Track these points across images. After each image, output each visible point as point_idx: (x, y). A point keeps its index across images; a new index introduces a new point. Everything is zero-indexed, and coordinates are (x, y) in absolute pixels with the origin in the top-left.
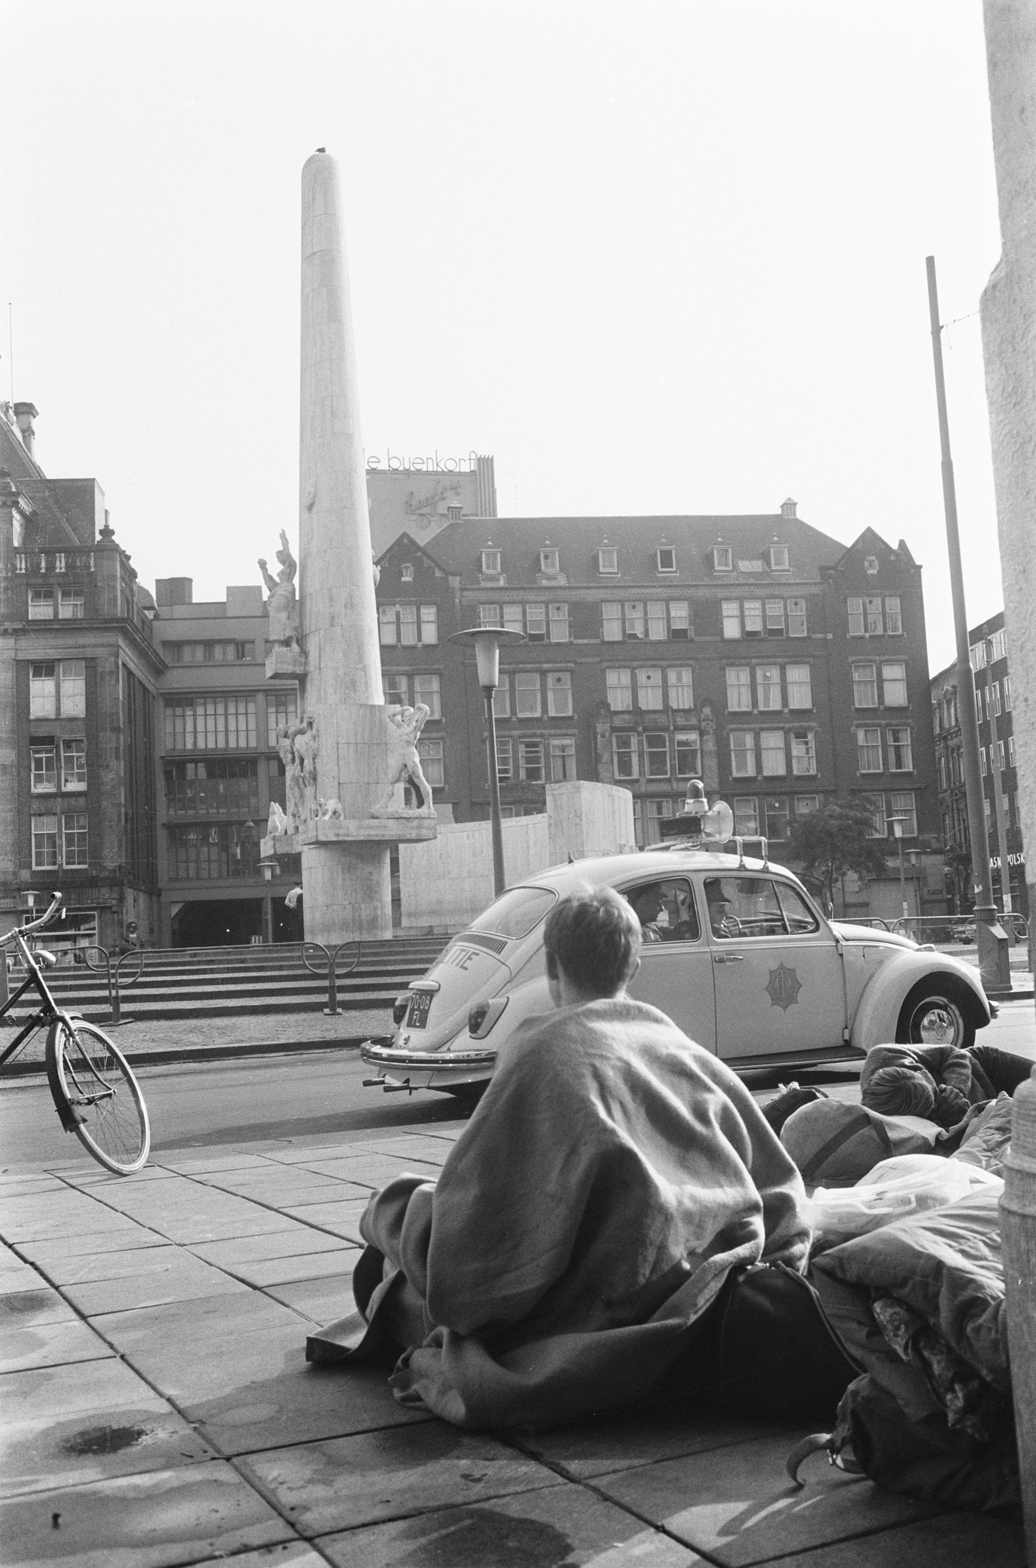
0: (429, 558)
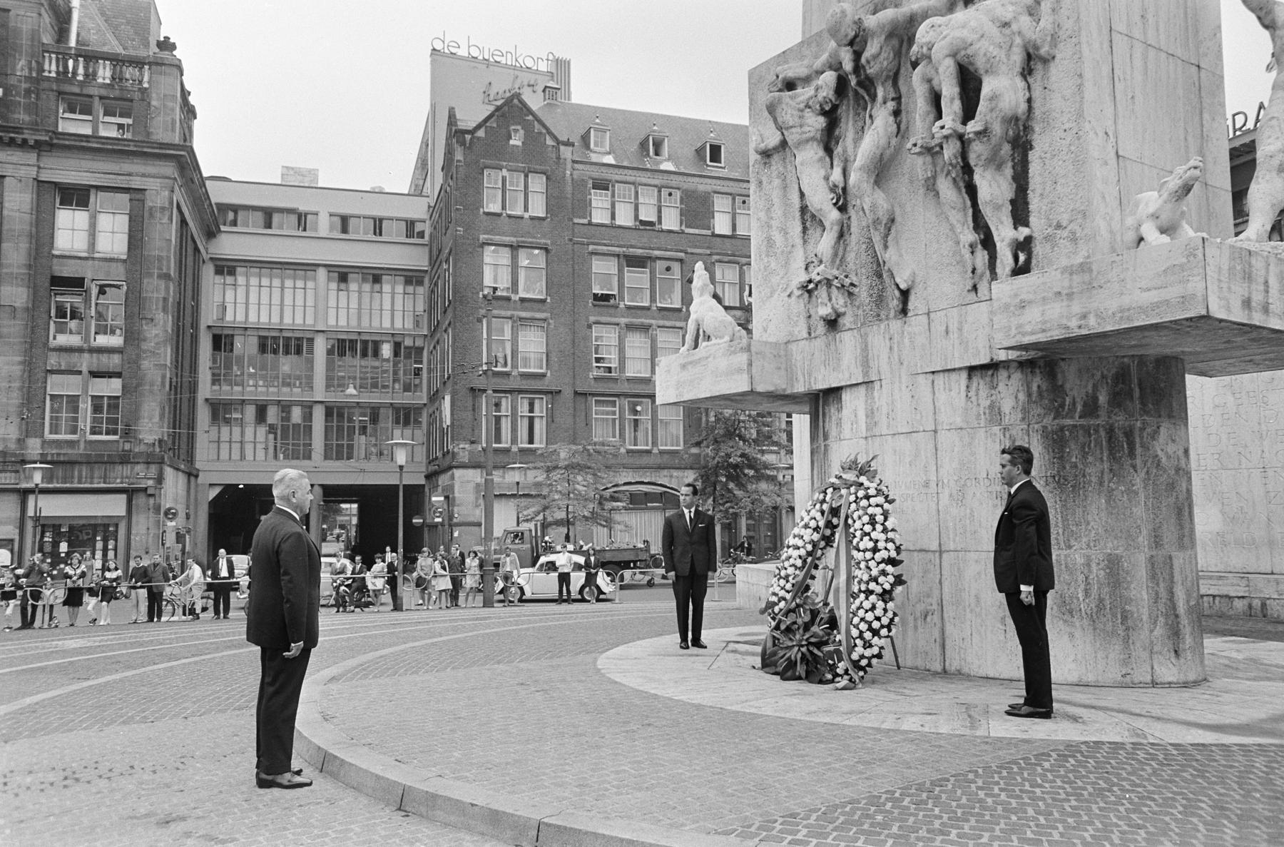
0: (540, 122)
